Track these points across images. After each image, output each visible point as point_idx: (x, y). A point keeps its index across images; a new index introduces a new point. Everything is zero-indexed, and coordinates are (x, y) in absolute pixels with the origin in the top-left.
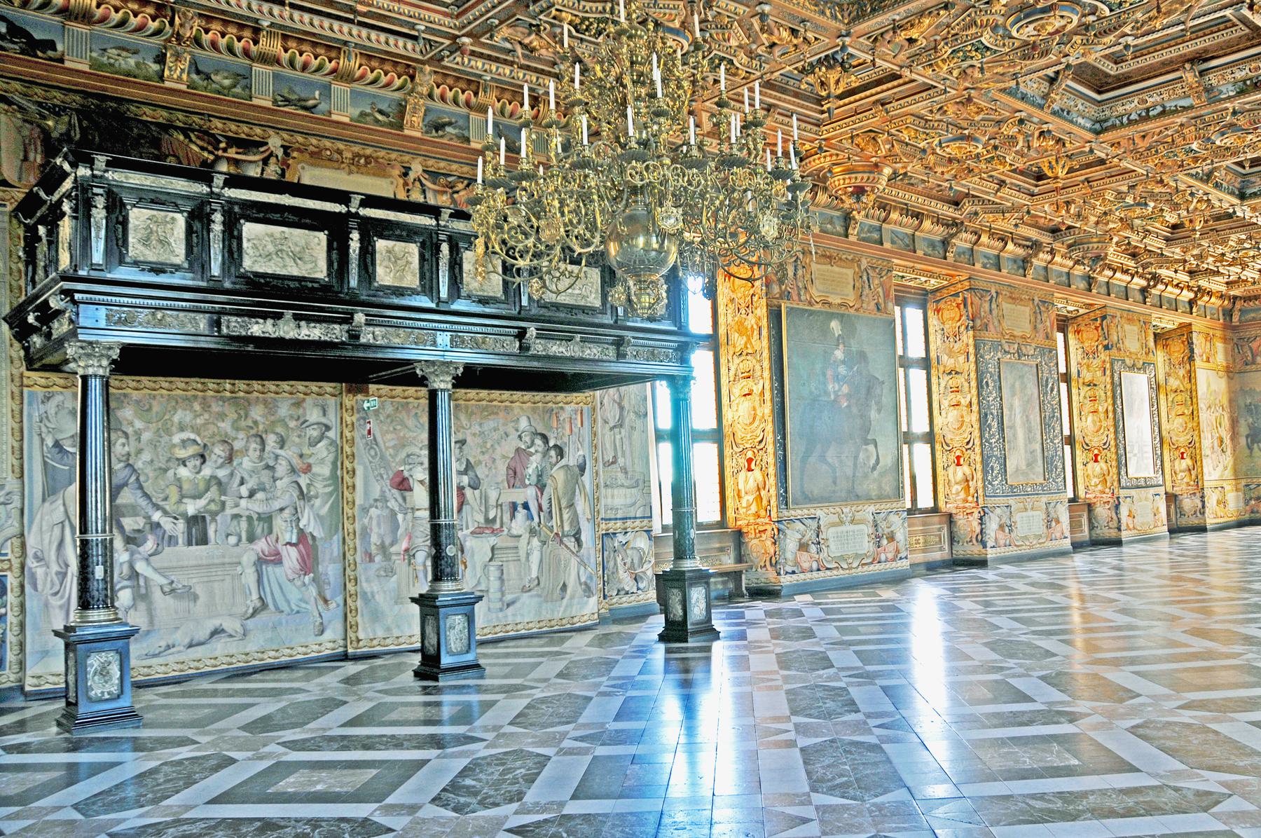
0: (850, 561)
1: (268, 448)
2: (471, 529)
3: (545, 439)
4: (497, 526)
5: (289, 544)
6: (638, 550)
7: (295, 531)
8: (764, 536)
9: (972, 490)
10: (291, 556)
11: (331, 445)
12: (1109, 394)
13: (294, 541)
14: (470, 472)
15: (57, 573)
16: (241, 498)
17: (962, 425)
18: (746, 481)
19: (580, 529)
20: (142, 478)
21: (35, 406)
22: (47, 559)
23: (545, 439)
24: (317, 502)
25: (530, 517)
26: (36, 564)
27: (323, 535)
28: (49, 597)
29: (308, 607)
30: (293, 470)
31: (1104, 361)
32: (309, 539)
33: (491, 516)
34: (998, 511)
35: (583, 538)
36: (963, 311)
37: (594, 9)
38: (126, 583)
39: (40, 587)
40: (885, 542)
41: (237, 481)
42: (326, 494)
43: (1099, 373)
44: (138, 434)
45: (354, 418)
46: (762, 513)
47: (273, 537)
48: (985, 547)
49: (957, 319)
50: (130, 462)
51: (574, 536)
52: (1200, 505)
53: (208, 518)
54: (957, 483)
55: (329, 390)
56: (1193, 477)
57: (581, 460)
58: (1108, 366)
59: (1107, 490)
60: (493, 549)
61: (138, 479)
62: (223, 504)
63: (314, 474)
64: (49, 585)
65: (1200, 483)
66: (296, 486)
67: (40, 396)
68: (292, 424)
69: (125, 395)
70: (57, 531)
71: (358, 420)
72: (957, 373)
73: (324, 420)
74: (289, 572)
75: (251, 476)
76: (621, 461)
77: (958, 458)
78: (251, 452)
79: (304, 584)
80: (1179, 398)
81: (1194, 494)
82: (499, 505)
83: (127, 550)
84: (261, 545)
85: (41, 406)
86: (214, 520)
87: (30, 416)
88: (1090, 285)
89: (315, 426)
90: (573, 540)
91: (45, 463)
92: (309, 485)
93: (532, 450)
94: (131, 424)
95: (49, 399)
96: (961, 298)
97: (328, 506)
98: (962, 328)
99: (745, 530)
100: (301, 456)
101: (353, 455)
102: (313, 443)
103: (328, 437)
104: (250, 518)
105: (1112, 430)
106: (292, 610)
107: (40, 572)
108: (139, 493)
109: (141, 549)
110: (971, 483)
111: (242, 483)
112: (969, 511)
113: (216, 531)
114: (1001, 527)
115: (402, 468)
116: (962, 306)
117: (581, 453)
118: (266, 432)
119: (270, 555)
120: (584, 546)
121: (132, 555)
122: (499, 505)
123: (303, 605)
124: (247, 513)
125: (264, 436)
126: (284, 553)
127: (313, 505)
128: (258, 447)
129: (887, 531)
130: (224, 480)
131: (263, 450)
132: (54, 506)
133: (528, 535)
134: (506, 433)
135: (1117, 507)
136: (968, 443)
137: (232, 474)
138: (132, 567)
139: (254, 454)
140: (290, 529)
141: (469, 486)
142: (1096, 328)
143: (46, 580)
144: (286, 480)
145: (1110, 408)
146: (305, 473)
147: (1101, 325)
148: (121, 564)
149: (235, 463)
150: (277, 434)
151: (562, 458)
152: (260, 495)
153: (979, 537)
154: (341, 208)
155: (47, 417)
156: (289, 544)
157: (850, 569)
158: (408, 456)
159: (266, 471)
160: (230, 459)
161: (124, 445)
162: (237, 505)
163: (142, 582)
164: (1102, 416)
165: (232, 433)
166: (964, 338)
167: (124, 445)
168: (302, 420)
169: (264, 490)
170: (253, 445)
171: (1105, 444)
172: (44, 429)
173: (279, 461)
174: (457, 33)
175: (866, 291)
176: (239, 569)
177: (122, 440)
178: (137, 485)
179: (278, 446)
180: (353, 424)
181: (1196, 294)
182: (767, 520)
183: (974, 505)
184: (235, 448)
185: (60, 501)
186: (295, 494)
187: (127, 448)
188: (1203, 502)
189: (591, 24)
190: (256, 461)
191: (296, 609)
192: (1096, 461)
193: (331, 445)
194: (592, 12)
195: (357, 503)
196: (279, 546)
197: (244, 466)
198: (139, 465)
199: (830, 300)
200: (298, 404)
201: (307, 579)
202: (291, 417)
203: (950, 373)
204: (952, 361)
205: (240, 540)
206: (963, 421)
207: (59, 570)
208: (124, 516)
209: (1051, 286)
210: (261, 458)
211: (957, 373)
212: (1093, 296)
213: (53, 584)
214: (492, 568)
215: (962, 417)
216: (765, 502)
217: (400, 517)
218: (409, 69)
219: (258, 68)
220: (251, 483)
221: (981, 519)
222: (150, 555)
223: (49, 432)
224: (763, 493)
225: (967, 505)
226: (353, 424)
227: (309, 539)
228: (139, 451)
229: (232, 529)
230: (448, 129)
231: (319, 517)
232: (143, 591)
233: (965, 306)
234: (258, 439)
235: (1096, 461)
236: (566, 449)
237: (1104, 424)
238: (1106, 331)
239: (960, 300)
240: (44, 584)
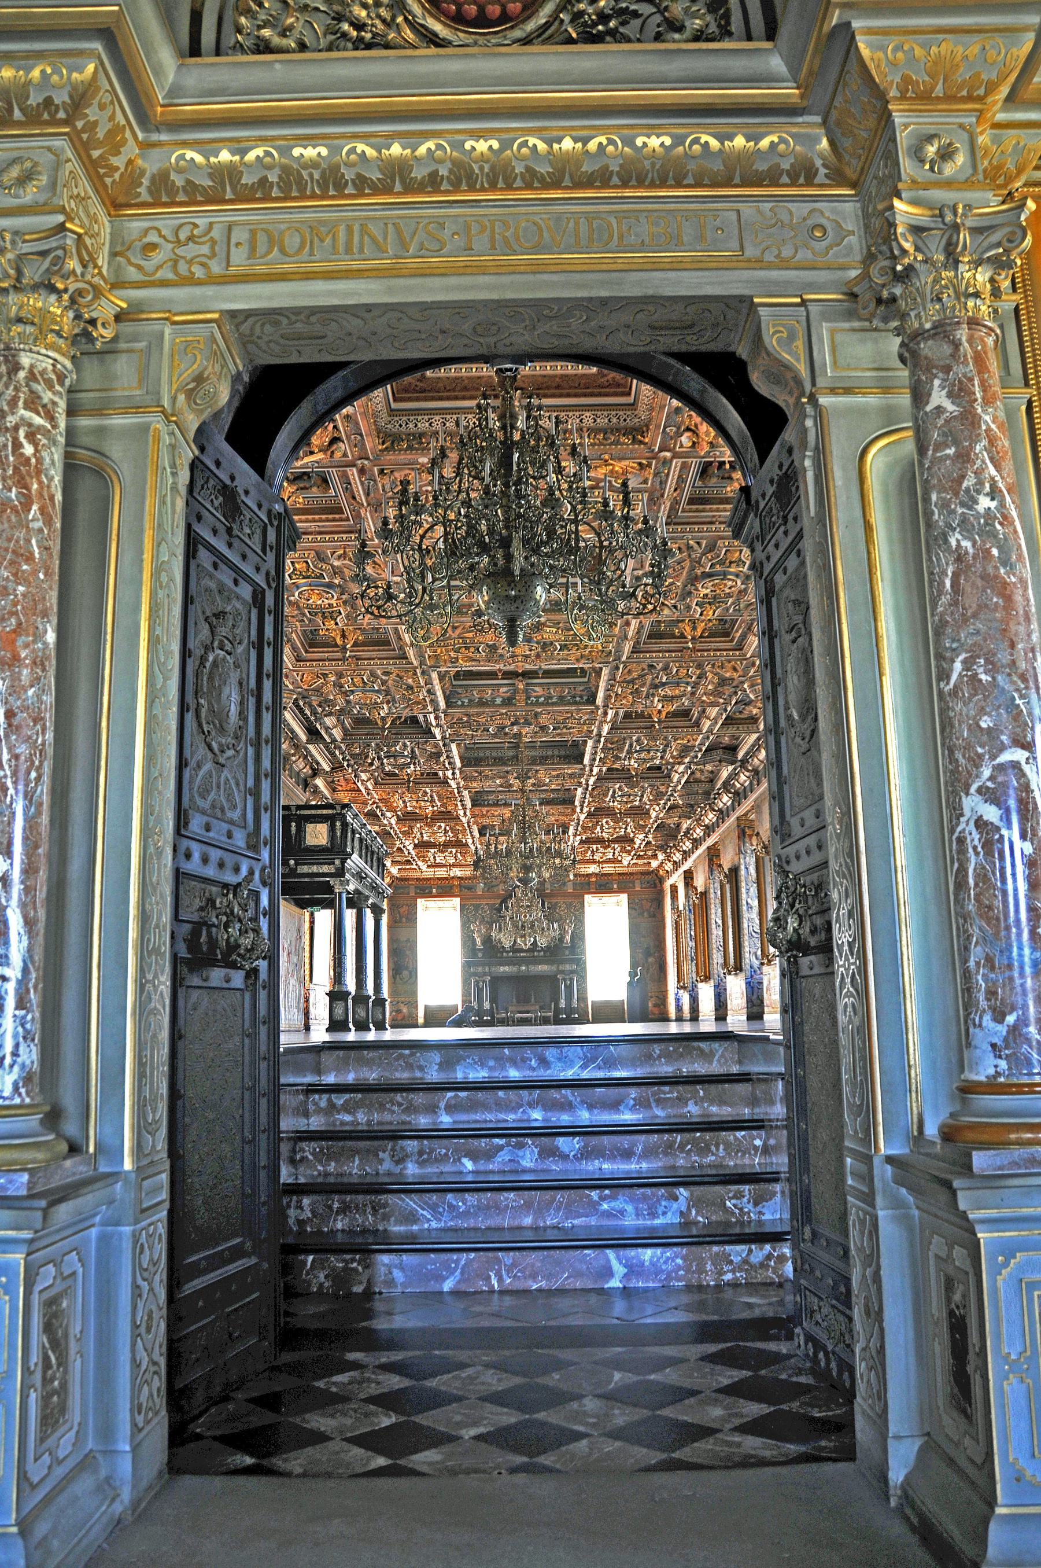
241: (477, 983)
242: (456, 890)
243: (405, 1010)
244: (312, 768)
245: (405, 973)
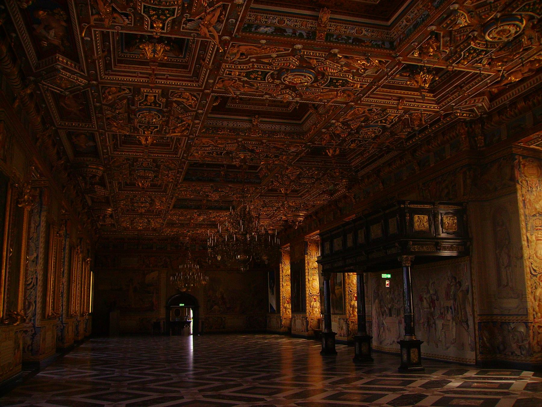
2: (437, 316)
3: (455, 278)
6: (520, 332)
14: (436, 294)
19: (468, 319)
23: (455, 278)
25: (452, 313)
76: (510, 284)
82: (444, 308)
93: (452, 284)
117: (467, 284)
120: (470, 327)
133: (452, 320)
151: (461, 287)
217: (421, 310)
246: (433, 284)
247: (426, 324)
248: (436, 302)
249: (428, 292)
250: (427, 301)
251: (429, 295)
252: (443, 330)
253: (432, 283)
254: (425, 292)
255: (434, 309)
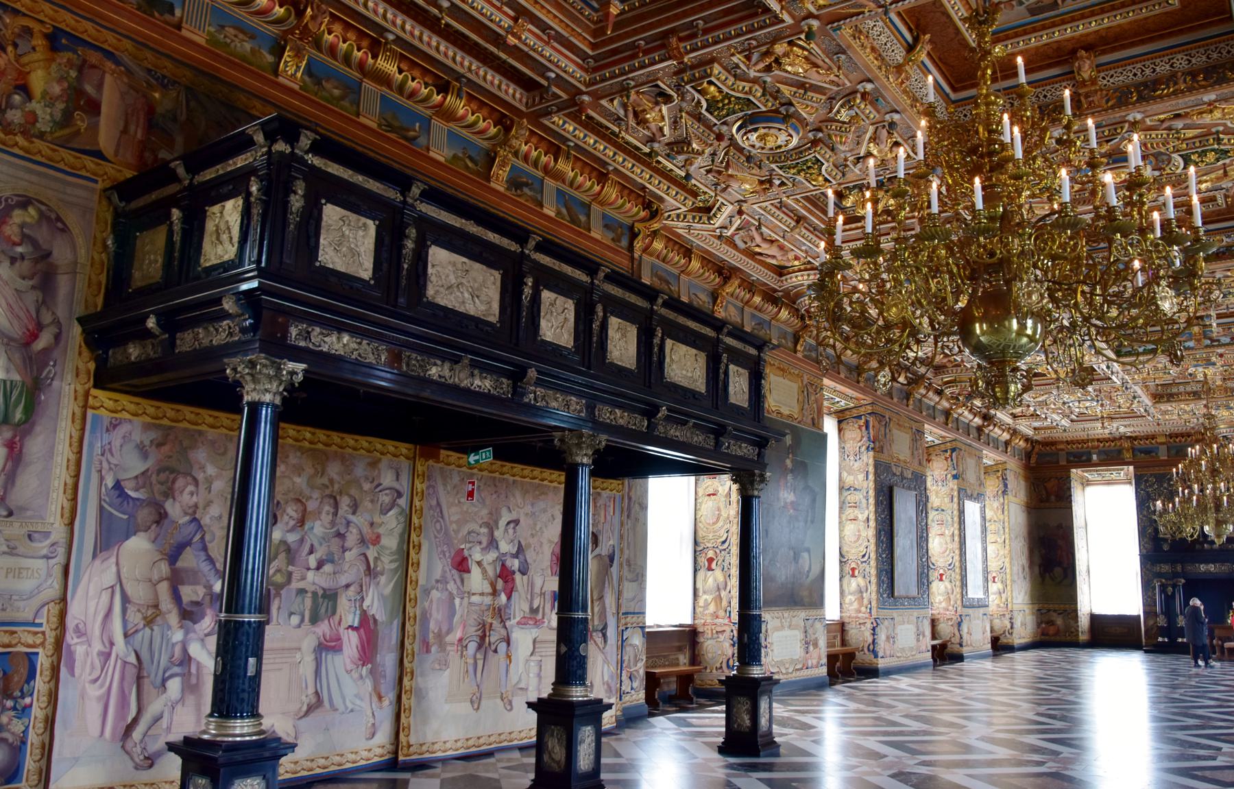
0: (787, 666)
1: (340, 512)
2: (518, 619)
4: (539, 617)
5: (351, 627)
7: (358, 612)
8: (722, 637)
9: (866, 601)
10: (351, 641)
11: (400, 514)
12: (956, 519)
13: (356, 625)
14: (520, 556)
15: (100, 654)
16: (309, 569)
17: (858, 539)
18: (705, 580)
19: (606, 624)
20: (207, 538)
21: (99, 435)
22: (89, 632)
24: (383, 579)
26: (76, 640)
27: (384, 618)
28: (87, 685)
29: (363, 704)
30: (363, 541)
31: (952, 489)
32: (371, 622)
33: (535, 606)
34: (886, 623)
35: (608, 634)
36: (865, 433)
37: (741, 88)
38: (176, 670)
39: (77, 671)
40: (811, 648)
41: (307, 548)
42: (391, 570)
43: (947, 500)
44: (209, 481)
45: (424, 486)
46: (721, 613)
47: (337, 618)
48: (876, 656)
49: (859, 439)
50: (197, 516)
51: (601, 630)
52: (1009, 627)
53: (273, 592)
54: (851, 594)
55: (404, 451)
56: (1003, 600)
57: (611, 551)
58: (956, 494)
59: (951, 608)
60: (534, 642)
61: (202, 538)
62: (290, 574)
63: (382, 547)
64: (88, 670)
65: (1009, 606)
66: (363, 559)
67: (106, 423)
68: (367, 486)
69: (200, 433)
70: (105, 597)
71: (428, 488)
72: (855, 489)
73: (396, 485)
74: (348, 661)
75: (321, 544)
77: (853, 570)
78: (323, 516)
79: (361, 677)
80: (993, 527)
81: (1004, 615)
82: (543, 594)
83: (181, 627)
84: (323, 628)
85: (105, 436)
86: (278, 594)
87: (91, 445)
88: (947, 419)
89: (387, 491)
90: (600, 635)
91: (101, 508)
92: (376, 559)
94: (202, 468)
95: (115, 426)
96: (863, 421)
97: (392, 585)
98: (863, 449)
99: (700, 630)
100: (372, 524)
101: (420, 527)
102: (384, 511)
103: (398, 505)
104: (315, 594)
105: (957, 552)
106: (347, 708)
107: (80, 651)
108: (202, 556)
109: (197, 627)
110: (865, 595)
111: (311, 552)
112: (862, 621)
113: (279, 608)
114: (888, 638)
115: (463, 547)
116: (864, 428)
117: (611, 542)
118: (341, 493)
119: (331, 640)
120: (609, 642)
121: (187, 633)
122: (543, 594)
123: (358, 702)
124: (312, 588)
125: (338, 497)
126: (345, 639)
127: (378, 583)
128: (332, 510)
129: (813, 637)
130: (293, 546)
131: (335, 514)
132: (106, 564)
134: (552, 516)
135: (959, 624)
136: (864, 556)
137: (302, 540)
138: (185, 650)
139: (326, 518)
140: (353, 609)
141: (519, 570)
142: (946, 459)
143: (86, 663)
144: (355, 552)
145: (957, 532)
146: (374, 545)
147: (951, 456)
148: (173, 645)
149: (306, 527)
150: (350, 496)
152: (328, 568)
153: (871, 647)
154: (514, 247)
155: (110, 450)
156: (351, 627)
157: (787, 673)
158: (469, 533)
159: (337, 539)
160: (302, 522)
161: (192, 494)
162: (303, 578)
163: (193, 670)
164: (948, 539)
165: (307, 492)
166: (865, 458)
167: (192, 494)
168: (376, 483)
169: (332, 562)
170: (327, 508)
171: (950, 565)
172: (105, 465)
173: (351, 529)
174: (584, 89)
175: (806, 406)
176: (298, 656)
177: (191, 488)
178: (200, 546)
179: (351, 511)
180: (423, 491)
181: (1012, 436)
182: (726, 621)
183: (867, 615)
184: (309, 509)
185: (113, 560)
186: (362, 568)
187: (195, 499)
188: (1012, 624)
189: (730, 102)
190: (328, 526)
191: (350, 706)
192: (941, 580)
193: (400, 514)
194: (738, 91)
195: (420, 583)
196: (341, 630)
197: (315, 531)
198: (206, 521)
199: (782, 411)
200: (374, 464)
201: (364, 671)
202: (367, 478)
203: (849, 489)
204: (852, 478)
205: (302, 621)
206: (860, 535)
207: (104, 650)
208: (183, 584)
209: (923, 417)
210: (333, 523)
211: (855, 489)
212: (949, 430)
213: (93, 668)
214: (532, 664)
215: (859, 531)
216: (725, 603)
217: (457, 601)
218: (505, 119)
219: (368, 84)
220: (320, 553)
221: (874, 629)
222: (206, 635)
223: (110, 469)
224: (723, 594)
225: (860, 615)
226: (423, 491)
227: (371, 622)
228: (208, 504)
229: (295, 608)
230: (526, 190)
231: (382, 596)
232: (194, 681)
233: (867, 428)
234: (332, 501)
235: (941, 580)
236: (600, 538)
237: (950, 546)
238: (955, 462)
239: (862, 422)
240: (83, 670)
241: (1163, 588)
242: (1128, 456)
243: (1059, 621)
244: (647, 205)
245: (1058, 571)
246: (512, 525)
247: (472, 646)
248: (518, 577)
249: (493, 543)
250: (484, 572)
251: (492, 555)
252: (532, 658)
253: (509, 523)
254: (480, 543)
255: (509, 598)
